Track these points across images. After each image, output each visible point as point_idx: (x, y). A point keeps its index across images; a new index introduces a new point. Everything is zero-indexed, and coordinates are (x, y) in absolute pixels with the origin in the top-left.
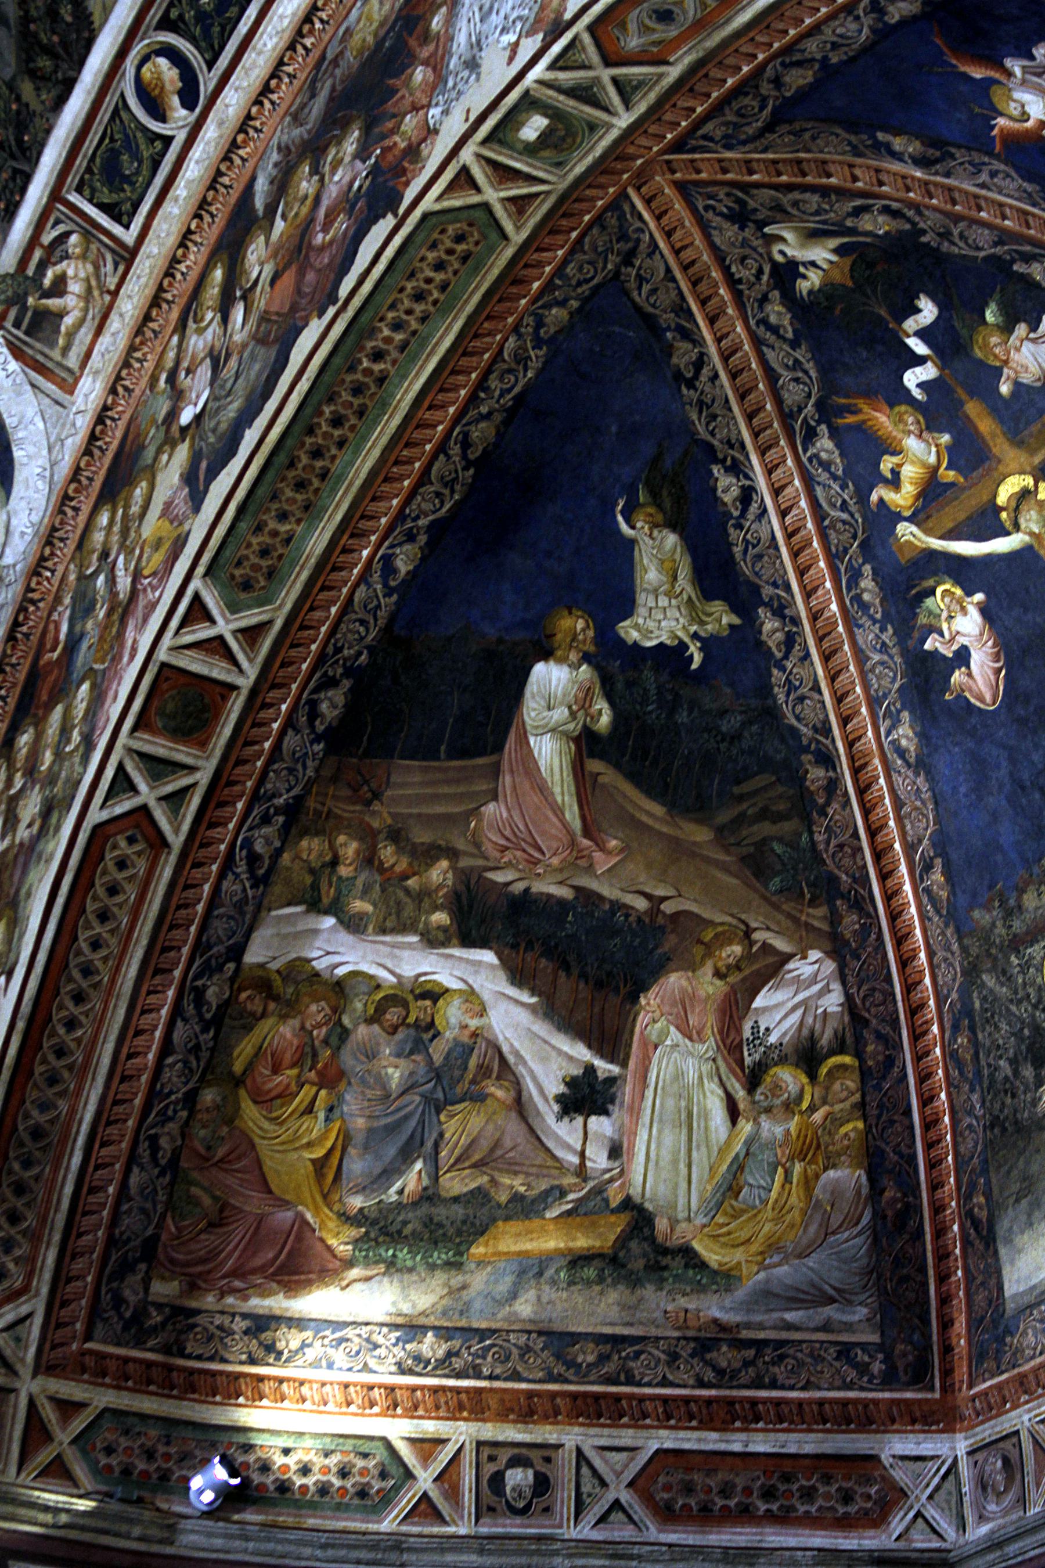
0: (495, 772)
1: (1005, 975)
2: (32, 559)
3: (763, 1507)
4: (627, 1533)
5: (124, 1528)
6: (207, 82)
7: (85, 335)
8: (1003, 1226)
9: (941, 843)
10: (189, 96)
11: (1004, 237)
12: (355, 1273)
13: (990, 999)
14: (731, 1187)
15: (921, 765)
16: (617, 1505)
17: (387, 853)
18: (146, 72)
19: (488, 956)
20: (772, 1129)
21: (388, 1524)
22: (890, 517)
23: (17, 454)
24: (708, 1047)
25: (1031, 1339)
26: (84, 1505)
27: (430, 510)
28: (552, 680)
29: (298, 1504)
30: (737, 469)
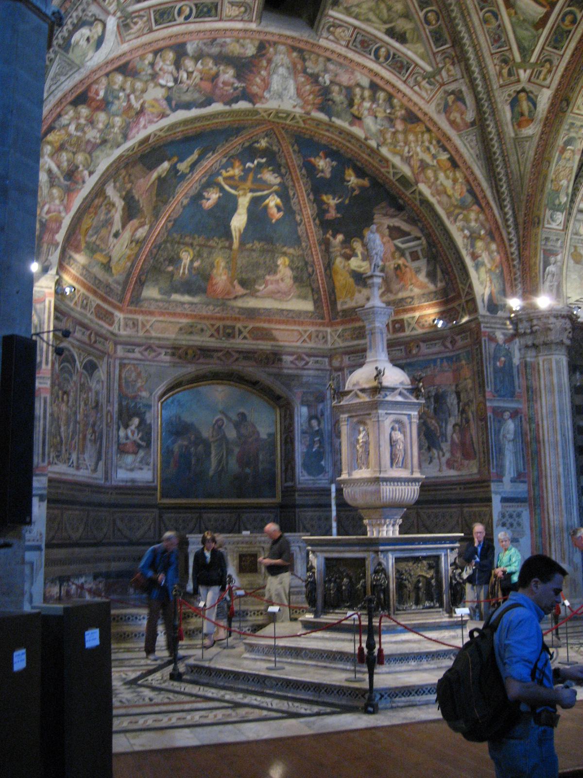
0: (147, 174)
1: (173, 246)
6: (191, 19)
7: (133, 36)
8: (147, 284)
9: (175, 220)
10: (187, 18)
11: (287, 164)
15: (184, 207)
17: (127, 178)
19: (123, 203)
21: (72, 305)
22: (221, 174)
24: (130, 234)
28: (166, 165)
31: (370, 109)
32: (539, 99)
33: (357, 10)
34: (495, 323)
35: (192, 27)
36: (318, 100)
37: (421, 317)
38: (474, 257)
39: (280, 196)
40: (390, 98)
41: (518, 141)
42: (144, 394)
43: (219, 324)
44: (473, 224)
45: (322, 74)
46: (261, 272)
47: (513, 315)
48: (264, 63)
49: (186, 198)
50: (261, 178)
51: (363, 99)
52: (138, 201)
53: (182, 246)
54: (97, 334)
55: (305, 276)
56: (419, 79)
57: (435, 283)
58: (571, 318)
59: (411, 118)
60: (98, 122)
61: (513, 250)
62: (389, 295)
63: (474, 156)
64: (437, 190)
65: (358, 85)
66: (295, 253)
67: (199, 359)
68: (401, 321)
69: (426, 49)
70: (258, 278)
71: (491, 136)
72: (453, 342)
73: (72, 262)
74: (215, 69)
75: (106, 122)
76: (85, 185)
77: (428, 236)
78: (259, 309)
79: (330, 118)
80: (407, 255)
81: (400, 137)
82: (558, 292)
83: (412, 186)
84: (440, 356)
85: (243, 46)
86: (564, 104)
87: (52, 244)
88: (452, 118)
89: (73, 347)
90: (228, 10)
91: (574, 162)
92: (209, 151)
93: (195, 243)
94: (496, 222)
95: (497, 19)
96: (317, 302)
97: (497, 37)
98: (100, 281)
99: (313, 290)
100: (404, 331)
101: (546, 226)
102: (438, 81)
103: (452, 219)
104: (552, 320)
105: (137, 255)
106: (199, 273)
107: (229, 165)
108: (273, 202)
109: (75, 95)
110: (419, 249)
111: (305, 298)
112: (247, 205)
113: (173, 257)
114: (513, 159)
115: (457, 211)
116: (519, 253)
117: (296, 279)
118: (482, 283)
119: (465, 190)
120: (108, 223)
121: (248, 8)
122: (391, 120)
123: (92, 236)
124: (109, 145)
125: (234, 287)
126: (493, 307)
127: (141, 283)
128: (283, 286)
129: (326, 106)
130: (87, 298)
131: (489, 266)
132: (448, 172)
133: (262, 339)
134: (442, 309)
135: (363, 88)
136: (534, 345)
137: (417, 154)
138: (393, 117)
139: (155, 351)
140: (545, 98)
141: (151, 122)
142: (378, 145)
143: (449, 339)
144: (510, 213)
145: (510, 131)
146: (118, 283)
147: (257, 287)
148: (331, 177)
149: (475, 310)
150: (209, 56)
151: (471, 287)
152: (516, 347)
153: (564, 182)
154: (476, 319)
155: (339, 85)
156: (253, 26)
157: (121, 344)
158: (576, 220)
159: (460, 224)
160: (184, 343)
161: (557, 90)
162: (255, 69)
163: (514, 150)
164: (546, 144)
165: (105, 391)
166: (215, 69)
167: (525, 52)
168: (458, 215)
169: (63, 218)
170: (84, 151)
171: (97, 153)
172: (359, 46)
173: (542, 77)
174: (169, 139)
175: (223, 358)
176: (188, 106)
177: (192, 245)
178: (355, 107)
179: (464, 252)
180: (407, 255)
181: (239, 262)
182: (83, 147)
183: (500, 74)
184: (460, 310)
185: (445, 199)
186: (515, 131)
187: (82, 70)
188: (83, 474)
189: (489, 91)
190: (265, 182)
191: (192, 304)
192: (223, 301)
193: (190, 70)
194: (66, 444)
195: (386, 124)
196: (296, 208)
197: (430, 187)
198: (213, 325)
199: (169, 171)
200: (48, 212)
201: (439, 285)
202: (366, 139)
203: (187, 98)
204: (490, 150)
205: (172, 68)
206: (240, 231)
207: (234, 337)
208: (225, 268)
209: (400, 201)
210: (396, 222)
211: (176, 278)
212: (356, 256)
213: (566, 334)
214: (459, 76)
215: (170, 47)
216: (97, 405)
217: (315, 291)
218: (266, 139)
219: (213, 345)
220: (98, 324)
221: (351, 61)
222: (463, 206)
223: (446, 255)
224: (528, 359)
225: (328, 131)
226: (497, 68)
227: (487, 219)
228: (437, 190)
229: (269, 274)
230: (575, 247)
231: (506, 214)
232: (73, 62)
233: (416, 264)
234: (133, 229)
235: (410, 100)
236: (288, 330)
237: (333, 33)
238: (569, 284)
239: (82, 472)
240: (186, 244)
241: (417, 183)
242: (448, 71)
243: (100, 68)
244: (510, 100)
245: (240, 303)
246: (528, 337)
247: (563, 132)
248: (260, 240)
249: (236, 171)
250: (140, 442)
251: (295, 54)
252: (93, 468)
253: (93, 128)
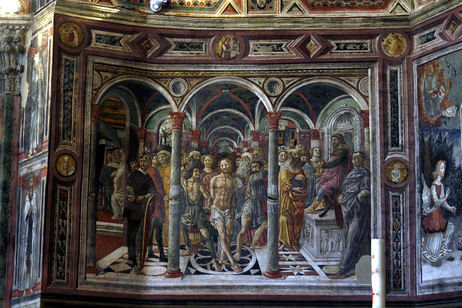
3: (345, 4)
4: (299, 14)
5: (129, 18)
16: (295, 5)
21: (218, 14)
26: (115, 11)
29: (187, 9)
42: (449, 112)
54: (325, 37)
89: (245, 78)
157: (418, 31)
165: (375, 126)
188: (293, 283)
194: (230, 238)
216: (343, 159)
239: (290, 280)
250: (448, 207)
252: (335, 270)
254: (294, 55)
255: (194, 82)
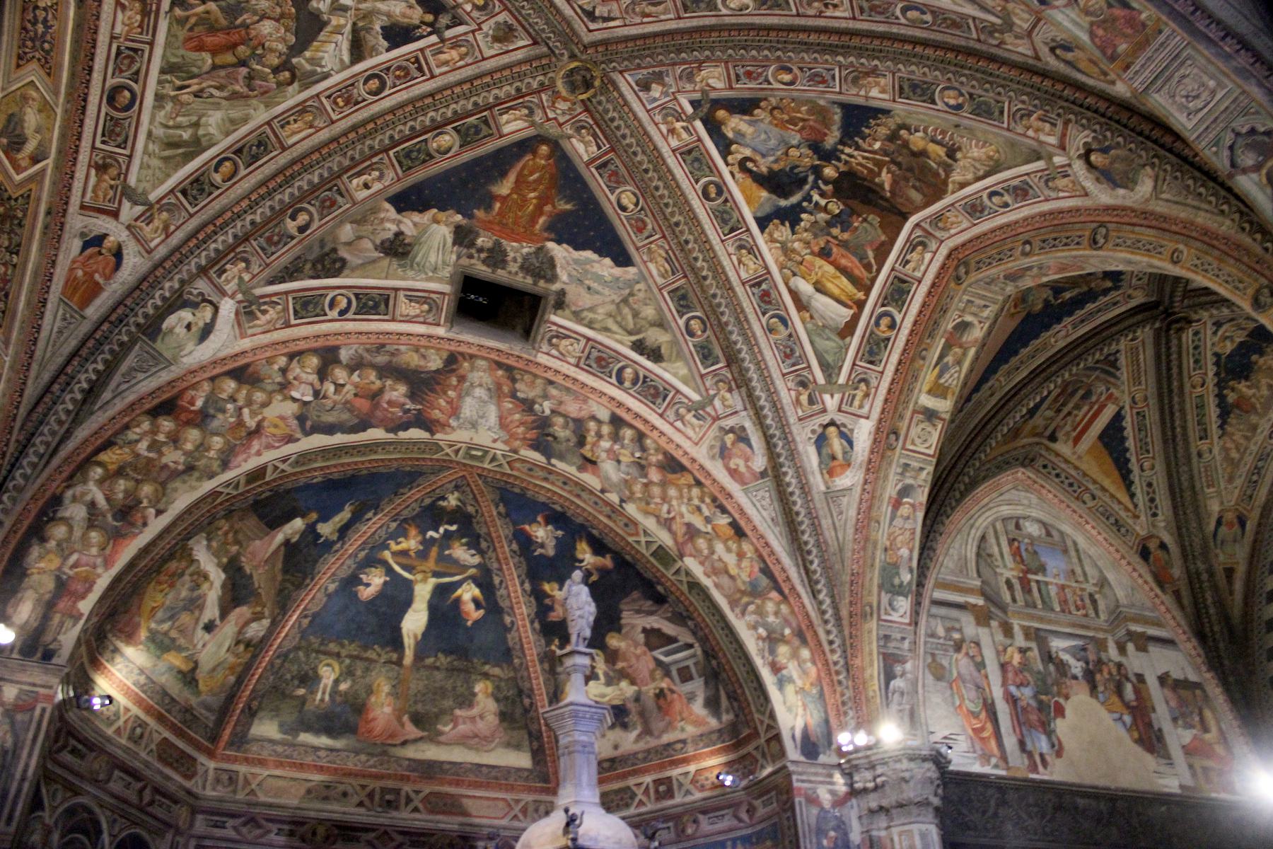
1: (307, 656)
2: (193, 368)
6: (349, 315)
7: (260, 330)
8: (260, 714)
9: (315, 616)
10: (342, 313)
11: (489, 534)
12: (141, 647)
13: (296, 660)
14: (214, 669)
15: (329, 596)
17: (231, 535)
18: (339, 298)
19: (223, 576)
20: (232, 659)
21: (110, 732)
22: (387, 547)
23: (212, 337)
24: (236, 629)
25: (255, 749)
27: (336, 476)
28: (298, 524)
30: (375, 514)
31: (609, 451)
32: (855, 435)
33: (591, 315)
34: (816, 774)
35: (350, 326)
36: (532, 434)
37: (698, 772)
38: (776, 668)
39: (479, 585)
40: (640, 437)
41: (832, 496)
43: (377, 784)
44: (771, 619)
45: (539, 400)
46: (448, 703)
47: (842, 761)
48: (454, 381)
49: (333, 582)
50: (450, 555)
51: (599, 436)
52: (251, 576)
53: (322, 657)
54: (156, 790)
55: (518, 711)
56: (682, 411)
57: (719, 718)
58: (939, 760)
59: (672, 465)
60: (186, 440)
61: (835, 657)
62: (648, 738)
63: (769, 521)
64: (713, 568)
65: (593, 418)
66: (502, 675)
67: (334, 843)
68: (669, 778)
69: (690, 370)
70: (443, 712)
71: (790, 489)
72: (751, 811)
73: (118, 659)
74: (378, 383)
75: (198, 443)
76: (147, 530)
77: (704, 640)
78: (443, 762)
79: (548, 459)
80: (674, 673)
81: (656, 490)
82: (912, 718)
83: (675, 561)
84: (732, 835)
85: (424, 357)
86: (893, 437)
87: (71, 616)
88: (732, 466)
89: (101, 806)
90: (405, 307)
91: (915, 521)
92: (369, 510)
93: (344, 653)
94: (807, 614)
95: (786, 326)
96: (538, 754)
97: (788, 351)
98: (173, 699)
99: (530, 734)
100: (672, 797)
101: (884, 617)
102: (709, 414)
103: (738, 610)
104: (905, 764)
105: (248, 667)
106: (346, 702)
107: (401, 532)
108: (468, 593)
109: (156, 401)
110: (690, 663)
111: (518, 747)
112: (428, 596)
113: (306, 674)
114: (826, 523)
115: (745, 599)
116: (846, 663)
117: (503, 716)
118: (789, 710)
119: (756, 569)
120: (194, 604)
121: (434, 307)
122: (642, 467)
123: (163, 621)
124: (196, 474)
125: (403, 725)
126: (810, 748)
127: (251, 714)
128: (481, 726)
129: (543, 441)
130: (143, 725)
131: (799, 683)
132: (730, 543)
133: (443, 813)
134: (731, 757)
135: (599, 422)
136: (881, 808)
137: (682, 516)
138: (643, 462)
139: (259, 826)
140: (863, 433)
141: (269, 447)
142: (622, 501)
143: (744, 808)
144: (828, 601)
145: (817, 482)
146: (208, 708)
147: (439, 727)
148: (556, 554)
149: (782, 753)
150: (373, 366)
151: (772, 716)
152: (852, 813)
153: (904, 552)
154: (785, 767)
155: (565, 416)
156: (441, 331)
157: (203, 812)
158: (930, 616)
159: (751, 618)
160: (312, 814)
161: (880, 421)
162: (438, 388)
163: (825, 505)
164: (873, 497)
166: (378, 383)
167: (830, 369)
168: (748, 604)
169: (99, 576)
170: (155, 480)
171: (177, 484)
172: (594, 365)
173: (856, 403)
174: (302, 480)
175: (376, 842)
176: (330, 430)
177: (338, 655)
178: (588, 447)
179: (758, 662)
180: (674, 673)
181: (413, 686)
182: (155, 474)
183: (798, 402)
184: (759, 757)
185: (725, 580)
186: (826, 483)
187: (173, 368)
189: (783, 425)
190: (456, 562)
191: (332, 750)
192: (382, 748)
193: (341, 382)
195: (634, 471)
196: (504, 604)
197: (702, 563)
198: (363, 787)
199: (304, 534)
200: (75, 565)
201: (727, 718)
202: (603, 491)
203: (329, 418)
204: (791, 510)
205: (313, 378)
206: (415, 636)
207: (397, 808)
208: (389, 694)
209: (660, 588)
210: (655, 622)
211: (309, 707)
212: (596, 677)
213: (933, 788)
214: (740, 407)
215: (314, 351)
217: (535, 736)
218: (456, 494)
219: (365, 819)
220: (161, 773)
221: (584, 385)
222: (754, 592)
223: (732, 669)
224: (874, 833)
225: (546, 479)
226: (793, 393)
227: (793, 612)
228: (713, 568)
229: (460, 706)
230: (933, 655)
231: (821, 603)
232: (161, 355)
233: (689, 687)
234: (241, 621)
235: (671, 441)
236: (488, 799)
237: (556, 347)
238: (929, 712)
240: (328, 654)
241: (681, 556)
242: (723, 400)
243: (203, 368)
244: (815, 437)
245: (411, 752)
246: (872, 796)
247: (893, 477)
248: (448, 652)
249: (411, 543)
251: (500, 373)
253: (176, 448)
254: (134, 798)
255: (69, 794)
